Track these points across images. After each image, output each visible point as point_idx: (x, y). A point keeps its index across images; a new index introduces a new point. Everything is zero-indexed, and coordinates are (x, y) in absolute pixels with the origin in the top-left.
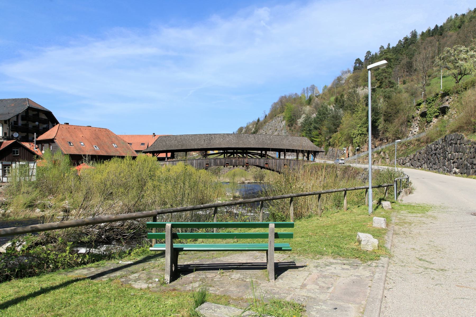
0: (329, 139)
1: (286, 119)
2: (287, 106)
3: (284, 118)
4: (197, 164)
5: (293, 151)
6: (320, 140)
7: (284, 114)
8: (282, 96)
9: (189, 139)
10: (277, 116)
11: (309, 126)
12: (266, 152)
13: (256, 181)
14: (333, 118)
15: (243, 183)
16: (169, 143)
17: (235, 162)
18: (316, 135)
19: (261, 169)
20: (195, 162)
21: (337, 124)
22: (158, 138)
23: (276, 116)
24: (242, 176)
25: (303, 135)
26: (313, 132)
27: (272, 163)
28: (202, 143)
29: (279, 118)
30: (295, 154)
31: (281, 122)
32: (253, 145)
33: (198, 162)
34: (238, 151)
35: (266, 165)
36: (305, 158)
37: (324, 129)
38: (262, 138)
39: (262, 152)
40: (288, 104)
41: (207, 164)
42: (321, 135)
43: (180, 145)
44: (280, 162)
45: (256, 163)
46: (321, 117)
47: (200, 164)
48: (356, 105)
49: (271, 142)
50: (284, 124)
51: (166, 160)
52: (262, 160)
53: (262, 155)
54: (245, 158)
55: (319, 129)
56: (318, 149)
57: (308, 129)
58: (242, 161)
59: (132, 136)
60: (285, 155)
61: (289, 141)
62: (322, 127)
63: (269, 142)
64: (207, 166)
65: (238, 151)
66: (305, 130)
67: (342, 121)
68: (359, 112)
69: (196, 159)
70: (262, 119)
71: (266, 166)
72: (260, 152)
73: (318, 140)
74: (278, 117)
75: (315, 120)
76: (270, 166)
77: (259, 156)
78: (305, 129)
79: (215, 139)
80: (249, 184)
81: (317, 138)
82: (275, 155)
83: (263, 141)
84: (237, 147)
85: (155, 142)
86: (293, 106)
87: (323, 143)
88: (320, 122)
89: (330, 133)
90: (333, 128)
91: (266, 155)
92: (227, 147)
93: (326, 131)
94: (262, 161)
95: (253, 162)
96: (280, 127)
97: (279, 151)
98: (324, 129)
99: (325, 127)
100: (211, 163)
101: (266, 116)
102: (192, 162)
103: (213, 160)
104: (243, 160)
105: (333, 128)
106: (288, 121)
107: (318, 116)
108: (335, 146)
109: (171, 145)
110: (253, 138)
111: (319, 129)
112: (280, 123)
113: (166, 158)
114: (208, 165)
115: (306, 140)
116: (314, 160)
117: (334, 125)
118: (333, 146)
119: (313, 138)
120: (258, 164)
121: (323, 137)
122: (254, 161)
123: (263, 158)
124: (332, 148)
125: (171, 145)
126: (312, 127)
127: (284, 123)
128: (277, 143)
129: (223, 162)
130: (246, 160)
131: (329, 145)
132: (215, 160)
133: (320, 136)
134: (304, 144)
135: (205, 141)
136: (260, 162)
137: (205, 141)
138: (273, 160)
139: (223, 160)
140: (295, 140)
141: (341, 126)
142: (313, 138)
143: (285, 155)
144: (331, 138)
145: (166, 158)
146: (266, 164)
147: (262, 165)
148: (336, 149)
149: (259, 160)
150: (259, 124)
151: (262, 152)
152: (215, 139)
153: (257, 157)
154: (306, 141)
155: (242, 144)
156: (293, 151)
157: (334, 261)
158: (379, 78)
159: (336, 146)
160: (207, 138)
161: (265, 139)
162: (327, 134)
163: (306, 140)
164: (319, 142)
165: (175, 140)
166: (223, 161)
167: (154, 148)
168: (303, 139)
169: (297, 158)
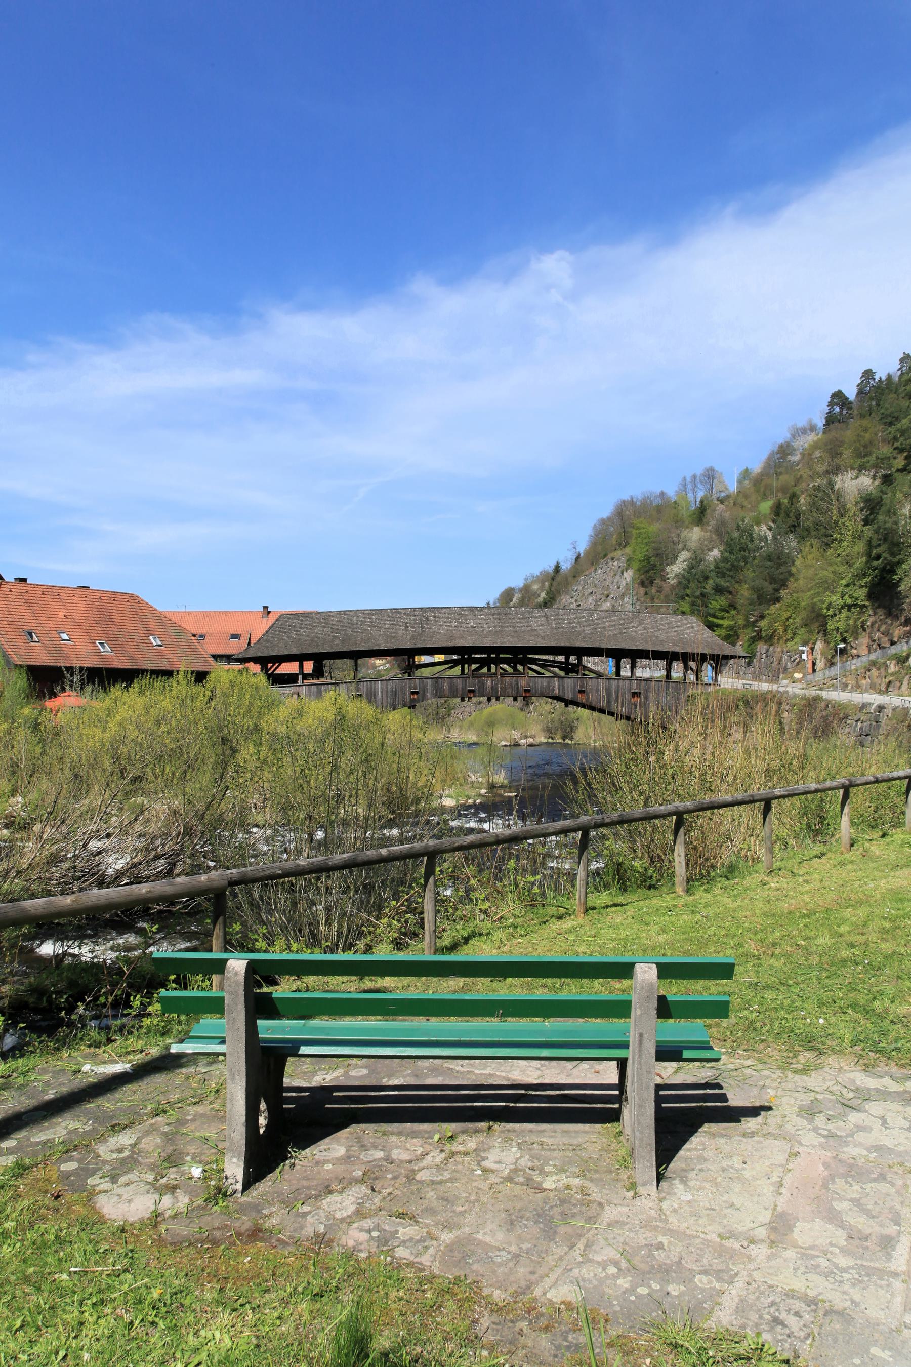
0: (756, 621)
1: (636, 565)
2: (638, 528)
3: (628, 561)
4: (387, 692)
5: (658, 655)
6: (732, 623)
7: (628, 550)
8: (624, 502)
9: (362, 623)
10: (610, 556)
11: (700, 585)
12: (580, 660)
13: (550, 740)
14: (770, 560)
15: (517, 745)
16: (307, 636)
18: (720, 609)
19: (566, 706)
21: (781, 577)
22: (277, 620)
23: (605, 556)
24: (514, 727)
25: (684, 609)
26: (713, 603)
27: (598, 690)
28: (400, 634)
29: (615, 564)
30: (662, 663)
31: (619, 573)
32: (543, 639)
34: (501, 656)
35: (580, 696)
36: (691, 677)
37: (744, 593)
38: (569, 620)
39: (567, 659)
40: (641, 522)
41: (413, 693)
42: (735, 608)
43: (337, 638)
45: (553, 690)
46: (733, 557)
47: (395, 694)
48: (836, 523)
49: (595, 630)
50: (628, 580)
51: (300, 682)
52: (569, 680)
53: (568, 668)
54: (522, 674)
55: (730, 593)
56: (727, 649)
57: (698, 593)
59: (206, 614)
60: (633, 667)
61: (645, 628)
62: (737, 586)
63: (587, 630)
64: (414, 699)
65: (501, 656)
66: (688, 595)
67: (794, 570)
68: (845, 544)
69: (383, 678)
70: (566, 566)
71: (581, 698)
72: (561, 658)
73: (726, 623)
74: (613, 559)
75: (717, 567)
76: (592, 698)
77: (561, 669)
78: (688, 592)
79: (436, 622)
80: (532, 748)
81: (723, 618)
82: (605, 666)
83: (574, 628)
84: (499, 643)
85: (267, 632)
86: (654, 527)
87: (739, 632)
88: (731, 574)
89: (760, 604)
90: (769, 588)
91: (581, 668)
92: (470, 643)
93: (748, 599)
94: (569, 686)
95: (542, 687)
96: (619, 588)
97: (617, 654)
98: (744, 593)
99: (747, 586)
100: (424, 691)
101: (578, 557)
102: (371, 687)
103: (430, 682)
104: (514, 683)
105: (769, 588)
106: (639, 570)
107: (726, 555)
108: (775, 641)
109: (312, 640)
110: (543, 620)
111: (730, 593)
112: (618, 577)
113: (300, 677)
115: (695, 625)
116: (716, 680)
117: (773, 580)
118: (769, 640)
119: (711, 619)
120: (556, 692)
121: (740, 617)
122: (545, 684)
123: (571, 675)
124: (765, 647)
125: (312, 640)
126: (709, 585)
127: (629, 575)
128: (610, 633)
129: (460, 686)
130: (523, 683)
131: (758, 638)
132: (437, 682)
133: (733, 612)
135: (407, 627)
136: (561, 688)
137: (407, 627)
138: (601, 681)
139: (460, 681)
140: (661, 624)
141: (792, 584)
142: (711, 619)
143: (633, 667)
144: (762, 617)
145: (300, 677)
146: (581, 692)
147: (569, 696)
148: (779, 649)
150: (558, 579)
151: (567, 659)
152: (436, 622)
153: (555, 674)
154: (693, 628)
155: (513, 637)
156: (658, 655)
157: (871, 1083)
158: (902, 444)
159: (779, 639)
160: (415, 620)
161: (576, 620)
162: (752, 607)
163: (695, 625)
164: (731, 628)
165: (324, 627)
166: (459, 683)
167: (267, 647)
168: (684, 621)
169: (668, 676)
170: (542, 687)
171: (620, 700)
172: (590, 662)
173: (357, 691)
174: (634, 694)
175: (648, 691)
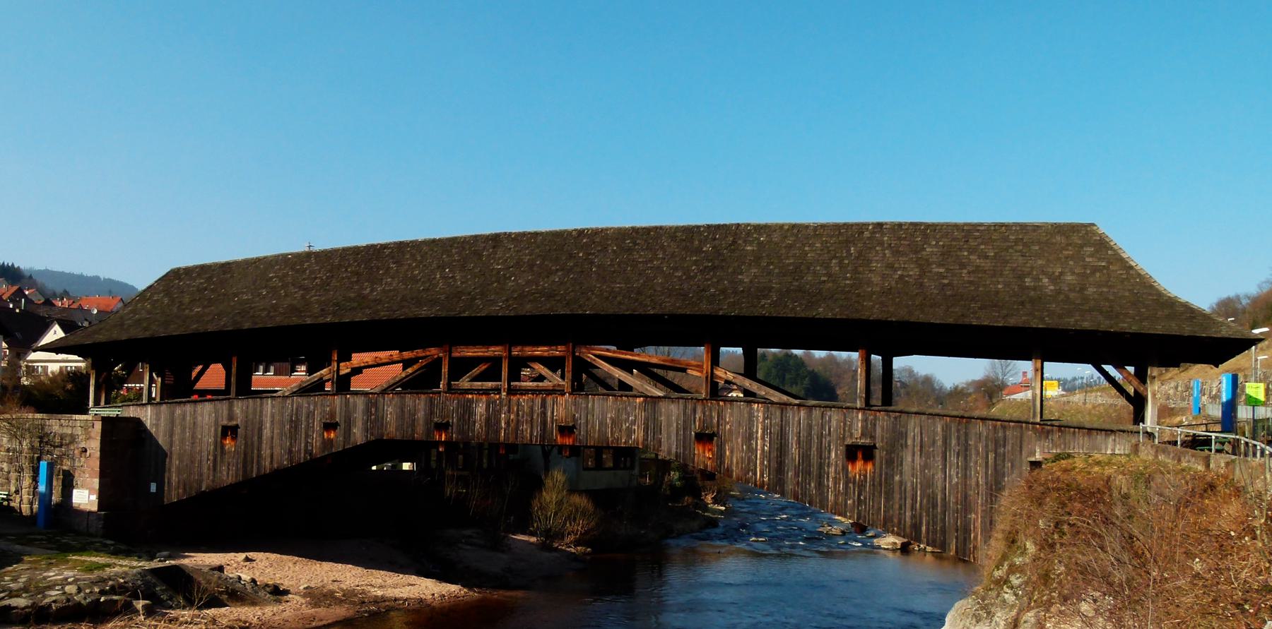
4: (282, 424)
17: (488, 420)
20: (273, 416)
27: (749, 437)
45: (630, 432)
64: (331, 441)
104: (537, 409)
129: (421, 415)
171: (814, 470)
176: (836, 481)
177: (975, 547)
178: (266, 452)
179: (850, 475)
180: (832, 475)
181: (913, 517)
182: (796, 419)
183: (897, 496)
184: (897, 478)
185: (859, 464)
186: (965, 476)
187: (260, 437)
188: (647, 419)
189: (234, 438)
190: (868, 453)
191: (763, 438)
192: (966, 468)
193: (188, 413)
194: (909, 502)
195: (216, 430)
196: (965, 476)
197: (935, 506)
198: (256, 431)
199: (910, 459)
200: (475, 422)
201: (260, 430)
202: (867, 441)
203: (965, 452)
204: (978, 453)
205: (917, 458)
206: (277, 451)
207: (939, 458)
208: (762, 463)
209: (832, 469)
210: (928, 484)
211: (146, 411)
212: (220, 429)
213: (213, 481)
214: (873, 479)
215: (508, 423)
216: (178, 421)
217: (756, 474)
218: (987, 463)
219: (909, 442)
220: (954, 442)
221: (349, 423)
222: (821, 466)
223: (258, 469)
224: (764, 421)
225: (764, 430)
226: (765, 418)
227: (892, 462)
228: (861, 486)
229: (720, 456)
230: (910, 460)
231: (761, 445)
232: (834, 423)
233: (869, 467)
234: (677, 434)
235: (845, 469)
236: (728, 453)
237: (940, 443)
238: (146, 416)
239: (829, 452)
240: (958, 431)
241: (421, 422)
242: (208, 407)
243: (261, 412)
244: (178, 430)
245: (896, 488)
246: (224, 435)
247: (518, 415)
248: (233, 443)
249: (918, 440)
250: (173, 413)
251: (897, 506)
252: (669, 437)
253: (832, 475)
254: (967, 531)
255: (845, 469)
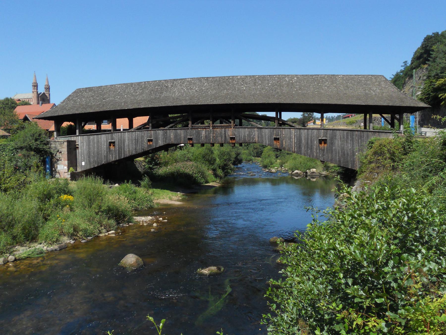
17: (206, 136)
27: (290, 138)
33: (134, 137)
35: (275, 142)
44: (308, 134)
45: (253, 138)
51: (77, 134)
52: (267, 130)
58: (221, 133)
64: (150, 145)
72: (272, 114)
95: (245, 136)
114: (151, 143)
122: (247, 133)
129: (182, 135)
132: (166, 133)
134: (374, 91)
138: (293, 131)
149: (259, 130)
154: (380, 85)
170: (245, 136)
172: (286, 116)
173: (112, 139)
174: (321, 141)
175: (333, 137)
176: (316, 149)
177: (356, 166)
178: (127, 149)
179: (321, 148)
180: (315, 148)
181: (339, 158)
182: (304, 132)
183: (334, 153)
184: (334, 148)
185: (323, 144)
186: (353, 147)
187: (124, 145)
188: (258, 134)
189: (114, 146)
190: (325, 141)
191: (294, 138)
192: (353, 144)
193: (95, 138)
194: (337, 154)
195: (107, 143)
196: (353, 147)
197: (344, 155)
198: (122, 144)
199: (337, 142)
200: (202, 137)
201: (124, 142)
202: (325, 138)
203: (352, 140)
204: (356, 140)
205: (339, 142)
206: (131, 149)
207: (345, 142)
208: (294, 145)
209: (315, 147)
210: (343, 149)
211: (78, 138)
212: (108, 143)
213: (107, 160)
214: (327, 148)
215: (213, 137)
216: (91, 141)
217: (292, 149)
218: (359, 142)
219: (337, 138)
220: (349, 137)
221: (157, 139)
222: (312, 146)
223: (124, 155)
224: (294, 134)
225: (294, 136)
226: (295, 133)
227: (332, 144)
228: (323, 150)
229: (282, 144)
230: (338, 143)
231: (294, 140)
232: (315, 133)
233: (326, 145)
234: (268, 138)
235: (319, 146)
236: (284, 143)
237: (345, 137)
238: (79, 140)
239: (314, 141)
240: (350, 134)
241: (183, 138)
242: (103, 136)
243: (124, 136)
244: (92, 143)
245: (334, 151)
246: (110, 145)
247: (216, 134)
248: (113, 147)
249: (339, 137)
250: (89, 139)
251: (334, 156)
252: (265, 139)
253: (315, 148)
254: (354, 161)
255: (319, 146)
